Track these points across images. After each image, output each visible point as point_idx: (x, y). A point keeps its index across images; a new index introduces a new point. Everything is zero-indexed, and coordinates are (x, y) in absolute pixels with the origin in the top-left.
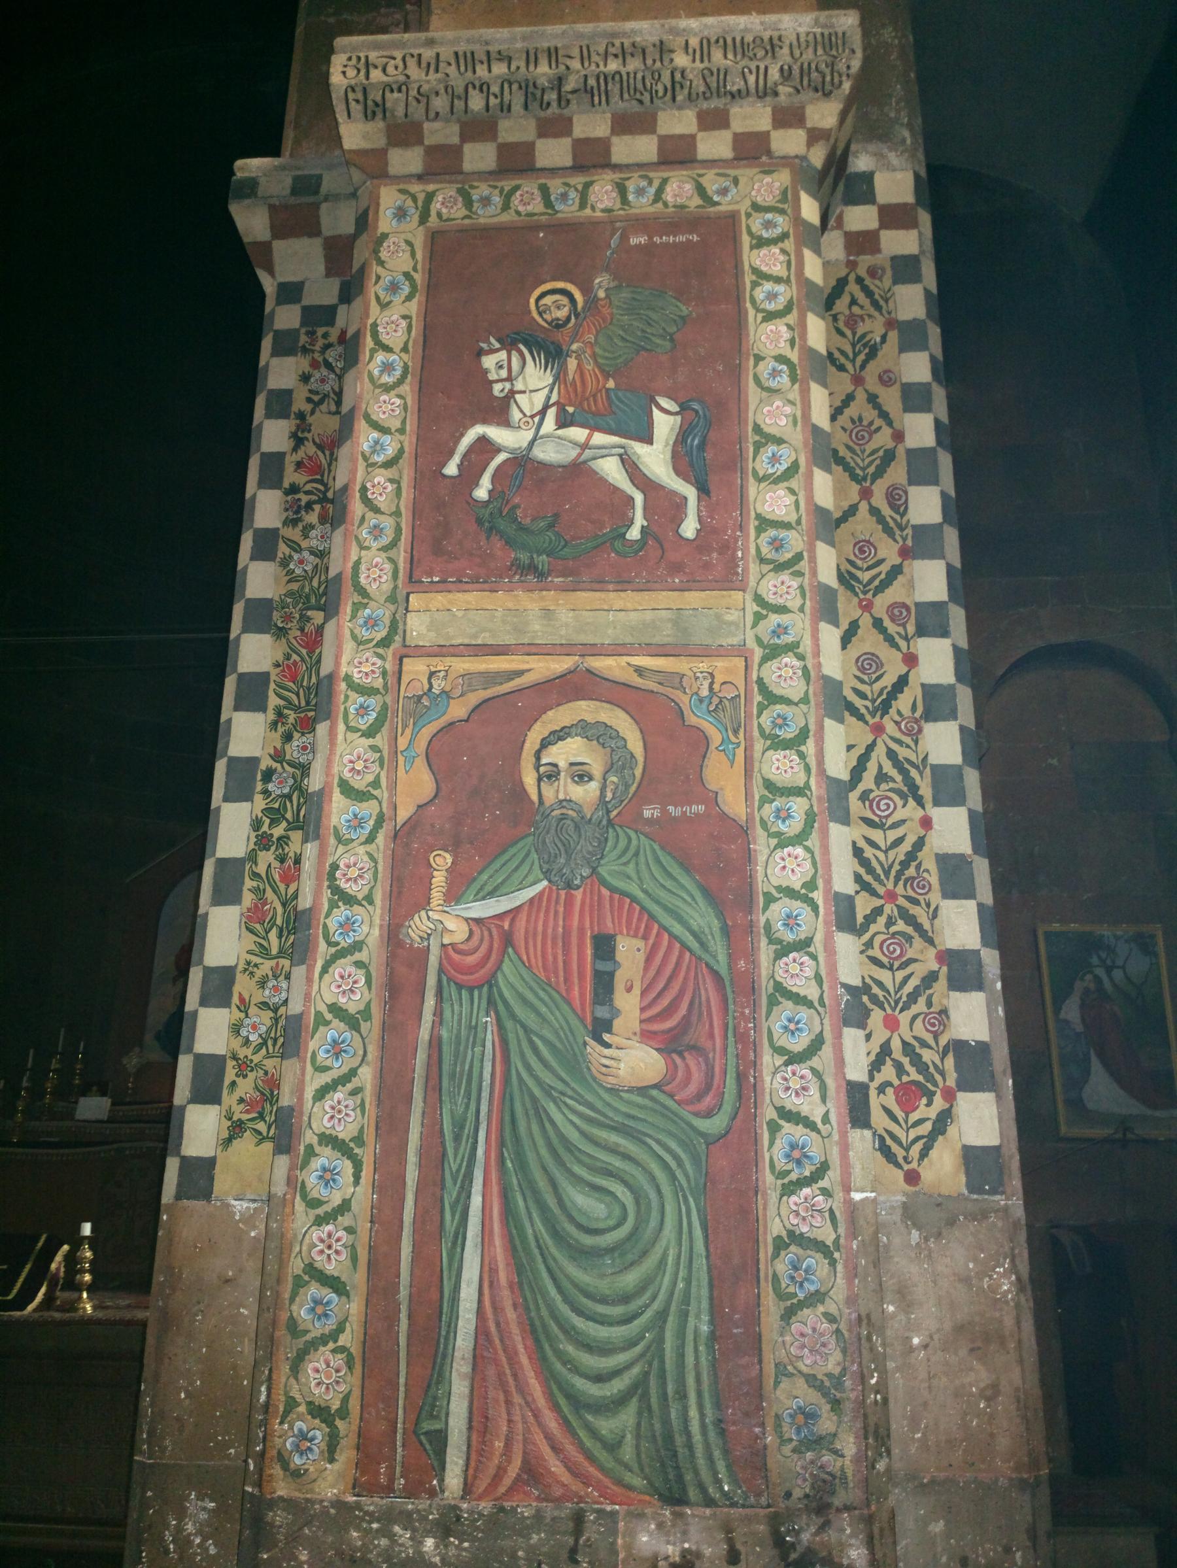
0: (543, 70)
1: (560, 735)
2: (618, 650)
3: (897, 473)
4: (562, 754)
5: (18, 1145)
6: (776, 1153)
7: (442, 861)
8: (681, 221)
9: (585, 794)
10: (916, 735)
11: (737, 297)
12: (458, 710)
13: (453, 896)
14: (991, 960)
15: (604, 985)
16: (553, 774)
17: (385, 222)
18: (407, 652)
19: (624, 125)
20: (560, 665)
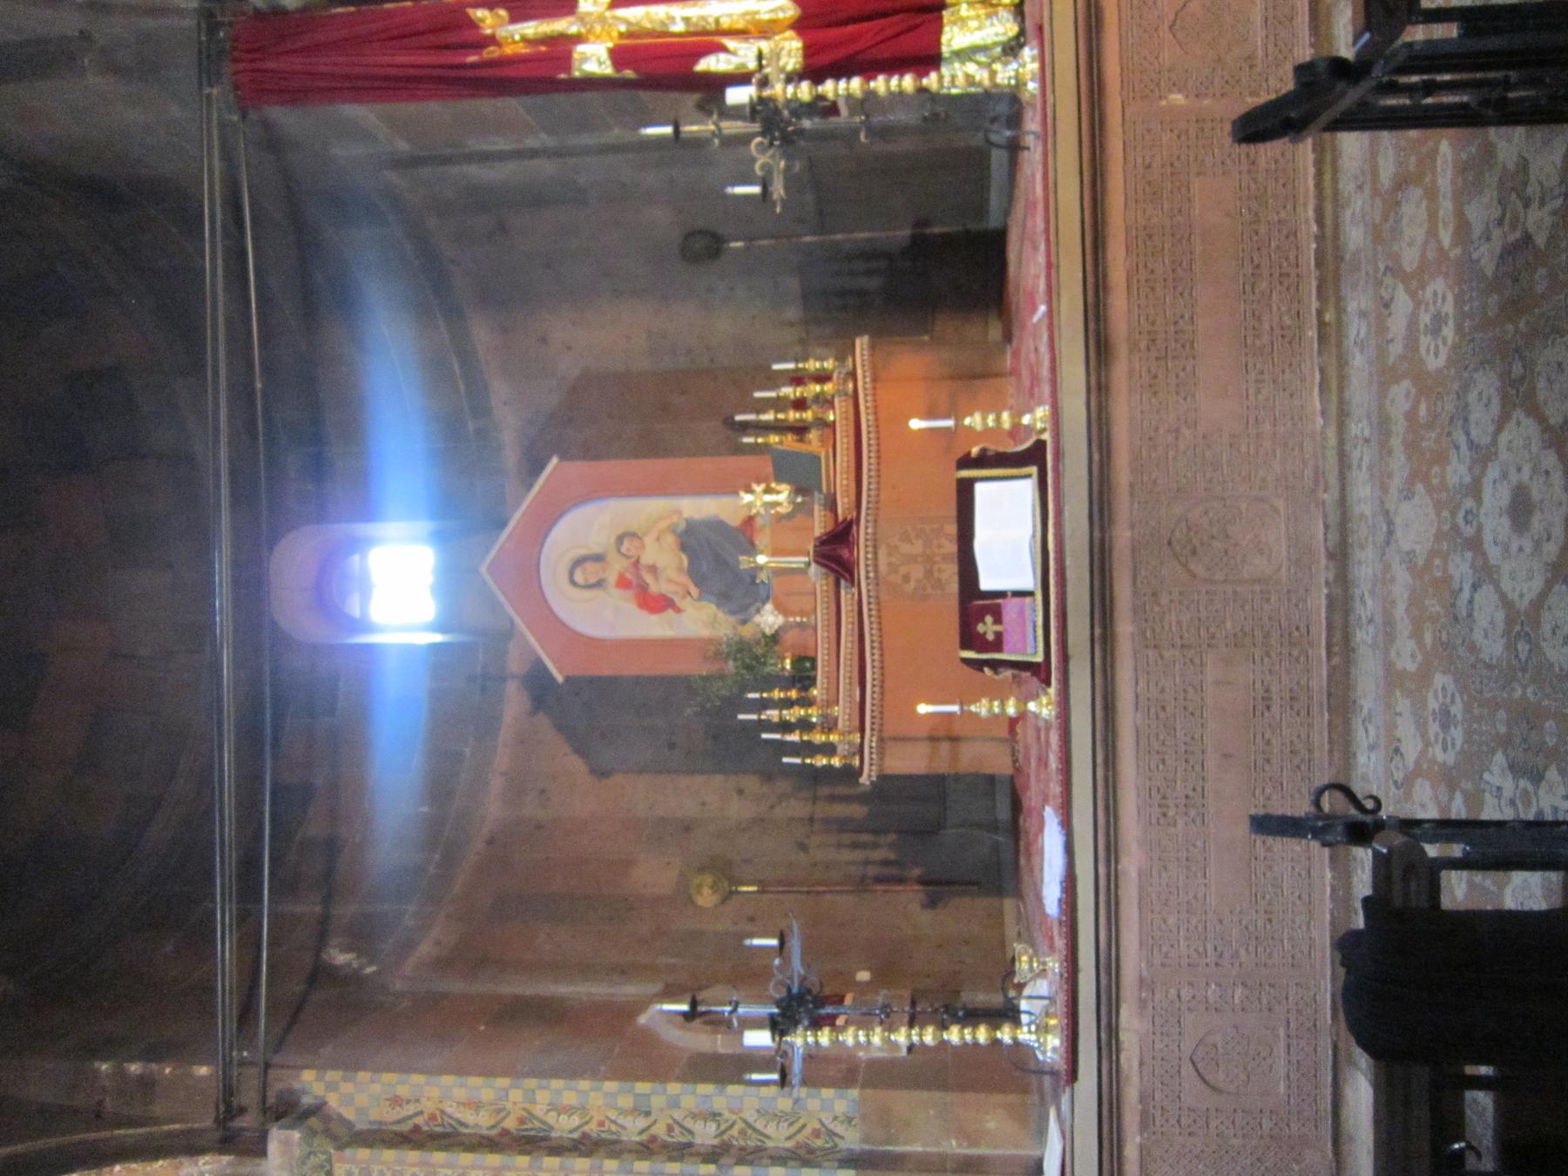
5: (862, 730)
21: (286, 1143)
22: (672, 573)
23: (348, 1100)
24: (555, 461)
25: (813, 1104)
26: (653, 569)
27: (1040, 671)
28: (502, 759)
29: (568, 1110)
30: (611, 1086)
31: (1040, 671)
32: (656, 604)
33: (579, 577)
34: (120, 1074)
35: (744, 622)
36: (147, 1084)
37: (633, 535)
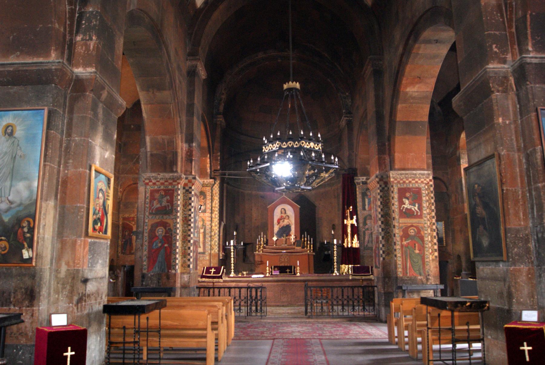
0: (407, 176)
1: (411, 230)
2: (414, 223)
3: (431, 205)
4: (412, 231)
6: (426, 257)
7: (404, 239)
8: (417, 188)
9: (413, 234)
10: (432, 226)
11: (421, 195)
12: (404, 228)
13: (405, 241)
14: (437, 243)
15: (415, 247)
16: (410, 232)
17: (394, 187)
18: (400, 223)
19: (413, 180)
20: (411, 224)
21: (212, 182)
22: (283, 224)
23: (216, 187)
24: (299, 207)
25: (217, 247)
26: (284, 221)
27: (272, 274)
28: (254, 192)
29: (215, 216)
30: (218, 221)
31: (272, 274)
32: (279, 222)
33: (283, 210)
34: (218, 156)
35: (276, 234)
36: (217, 160)
37: (289, 218)
